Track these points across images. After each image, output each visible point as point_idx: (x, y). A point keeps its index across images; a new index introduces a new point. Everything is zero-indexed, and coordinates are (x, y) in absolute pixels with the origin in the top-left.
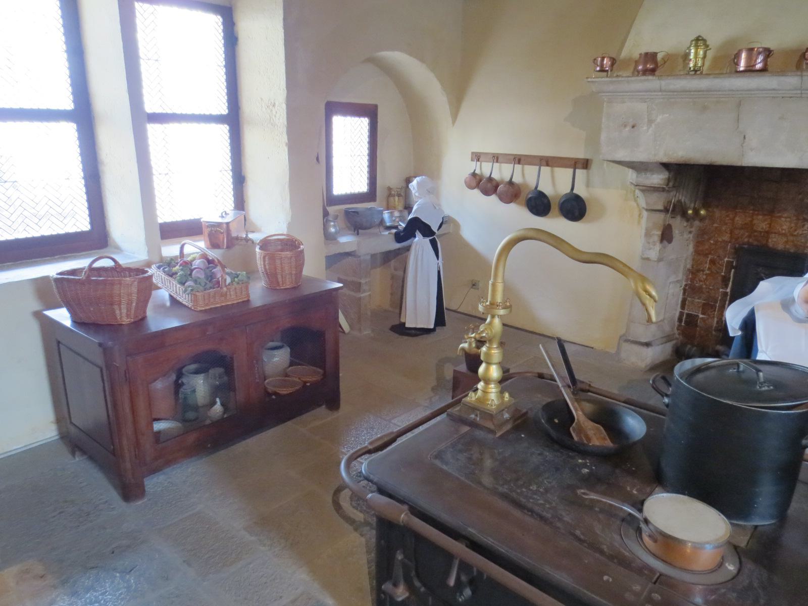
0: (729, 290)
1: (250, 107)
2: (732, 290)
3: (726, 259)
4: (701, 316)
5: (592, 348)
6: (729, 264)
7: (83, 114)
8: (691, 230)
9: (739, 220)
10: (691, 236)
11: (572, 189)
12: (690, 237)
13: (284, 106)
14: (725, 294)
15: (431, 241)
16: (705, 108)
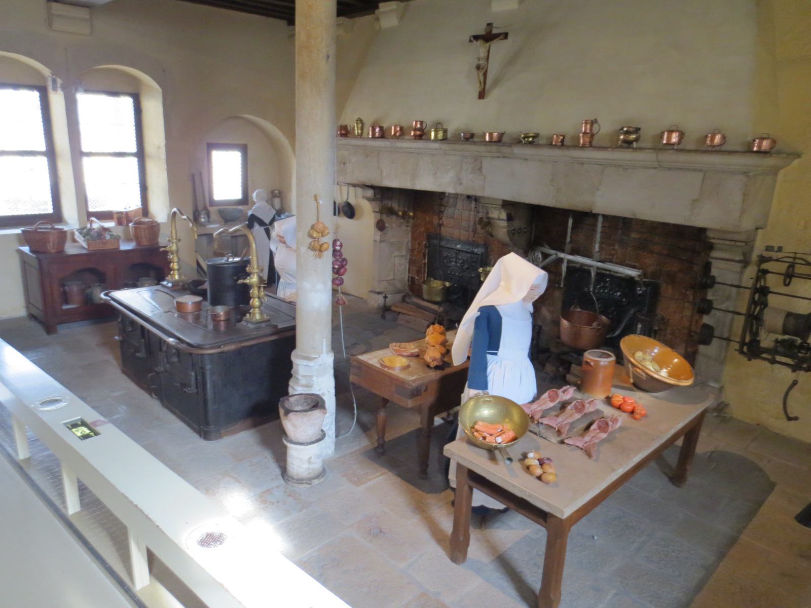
0: (426, 261)
1: (149, 148)
2: (428, 261)
3: (424, 242)
4: (417, 278)
5: (362, 298)
6: (425, 245)
7: (51, 153)
8: (408, 224)
9: (428, 218)
10: (409, 229)
11: (347, 199)
12: (407, 229)
13: (164, 149)
14: (425, 263)
15: (265, 229)
16: (367, 156)
